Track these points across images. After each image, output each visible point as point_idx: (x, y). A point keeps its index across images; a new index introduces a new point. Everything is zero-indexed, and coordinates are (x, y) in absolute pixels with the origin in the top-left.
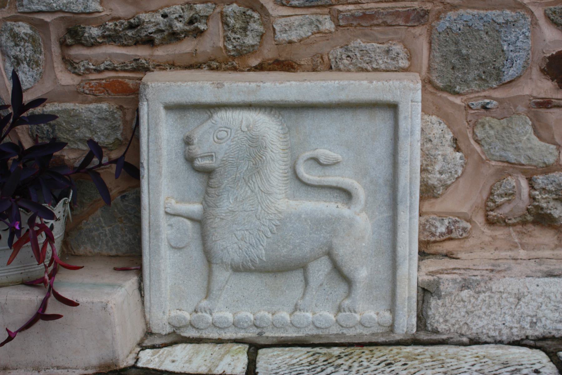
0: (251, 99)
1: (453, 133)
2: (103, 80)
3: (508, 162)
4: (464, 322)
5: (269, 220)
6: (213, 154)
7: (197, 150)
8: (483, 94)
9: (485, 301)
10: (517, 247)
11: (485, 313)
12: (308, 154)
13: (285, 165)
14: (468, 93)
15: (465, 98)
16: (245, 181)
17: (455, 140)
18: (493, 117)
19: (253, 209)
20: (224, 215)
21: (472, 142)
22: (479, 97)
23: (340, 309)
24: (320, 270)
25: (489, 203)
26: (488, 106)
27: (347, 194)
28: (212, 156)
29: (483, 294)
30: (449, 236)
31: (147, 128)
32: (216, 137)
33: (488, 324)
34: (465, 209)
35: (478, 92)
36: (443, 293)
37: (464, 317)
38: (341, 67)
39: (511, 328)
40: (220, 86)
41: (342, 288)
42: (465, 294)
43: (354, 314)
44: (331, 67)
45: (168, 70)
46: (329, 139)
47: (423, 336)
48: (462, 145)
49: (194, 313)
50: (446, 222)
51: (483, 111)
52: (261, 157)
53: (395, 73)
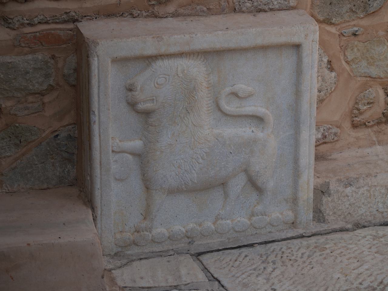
0: (186, 49)
1: (329, 57)
2: (36, 32)
3: (370, 77)
4: (348, 212)
5: (200, 149)
6: (154, 98)
7: (139, 95)
8: (353, 23)
9: (364, 194)
10: (375, 144)
11: (363, 203)
12: (228, 90)
13: (209, 100)
14: (341, 23)
15: (339, 27)
16: (181, 118)
17: (329, 62)
18: (359, 41)
19: (187, 141)
20: (164, 148)
21: (344, 63)
22: (349, 25)
24: (238, 184)
25: (354, 111)
26: (356, 34)
27: (259, 119)
28: (153, 99)
29: (362, 189)
30: (324, 141)
31: (97, 80)
32: (158, 84)
33: (366, 212)
34: (337, 118)
35: (349, 21)
36: (332, 192)
37: (348, 208)
38: (244, 9)
39: (382, 213)
41: (254, 196)
43: (264, 217)
44: (235, 9)
45: (95, 19)
48: (335, 66)
49: (136, 234)
51: (353, 37)
52: (194, 97)
53: (287, 11)
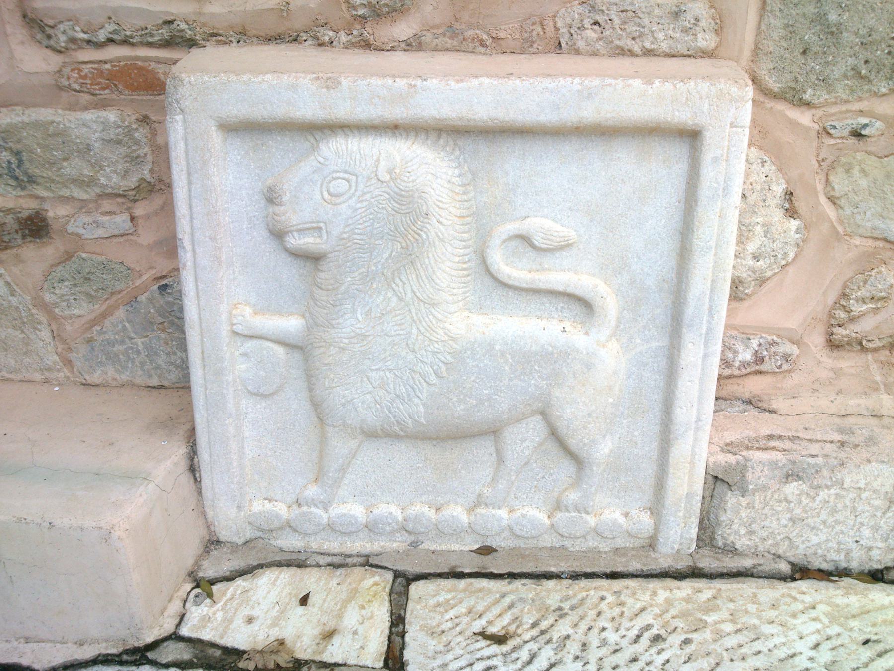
0: (397, 113)
1: (787, 183)
2: (105, 62)
3: (885, 240)
4: (785, 535)
5: (433, 353)
6: (322, 225)
7: (292, 215)
8: (857, 106)
9: (828, 502)
10: (877, 389)
11: (824, 522)
12: (511, 227)
13: (465, 247)
14: (827, 104)
15: (819, 113)
16: (386, 279)
17: (789, 195)
18: (869, 153)
19: (401, 332)
20: (346, 341)
21: (823, 200)
22: (848, 111)
23: (558, 506)
24: (526, 438)
25: (837, 312)
26: (863, 132)
27: (583, 305)
28: (320, 228)
29: (826, 491)
30: (757, 368)
31: (185, 169)
33: (828, 540)
34: (793, 323)
35: (847, 102)
36: (751, 487)
37: (786, 526)
38: (581, 44)
39: (870, 549)
40: (332, 84)
41: (565, 470)
42: (792, 489)
43: (583, 515)
44: (560, 44)
45: (235, 44)
46: (552, 194)
47: (707, 562)
48: (801, 205)
49: (295, 507)
50: (755, 344)
51: (853, 140)
52: (418, 234)
53: (689, 60)
